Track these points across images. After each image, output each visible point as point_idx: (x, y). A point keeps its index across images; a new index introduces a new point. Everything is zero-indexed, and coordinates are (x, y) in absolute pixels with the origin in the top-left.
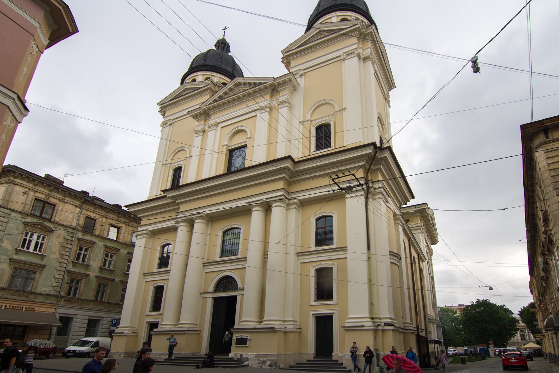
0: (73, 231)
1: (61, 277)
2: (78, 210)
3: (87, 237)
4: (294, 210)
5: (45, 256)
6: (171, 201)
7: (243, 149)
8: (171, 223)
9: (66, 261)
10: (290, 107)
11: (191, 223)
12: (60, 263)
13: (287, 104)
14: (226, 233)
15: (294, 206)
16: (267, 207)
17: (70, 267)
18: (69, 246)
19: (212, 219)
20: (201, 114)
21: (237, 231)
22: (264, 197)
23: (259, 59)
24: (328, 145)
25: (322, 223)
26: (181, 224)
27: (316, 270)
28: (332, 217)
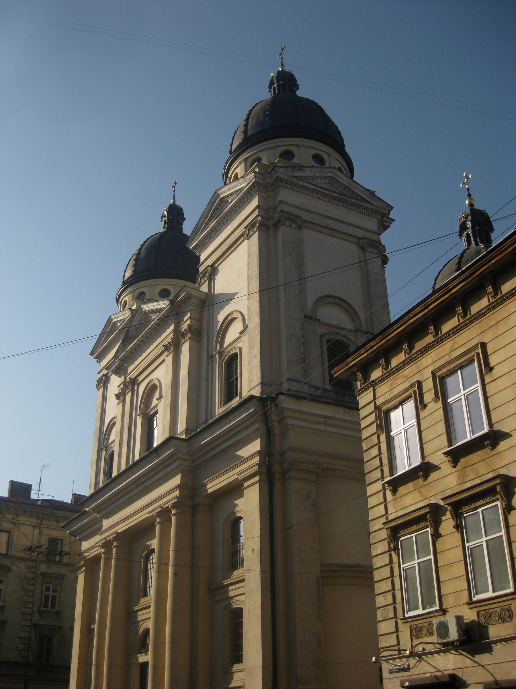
0: (34, 564)
1: (27, 635)
2: (37, 531)
3: (54, 569)
5: (5, 607)
9: (30, 611)
12: (24, 614)
17: (36, 618)
18: (32, 588)
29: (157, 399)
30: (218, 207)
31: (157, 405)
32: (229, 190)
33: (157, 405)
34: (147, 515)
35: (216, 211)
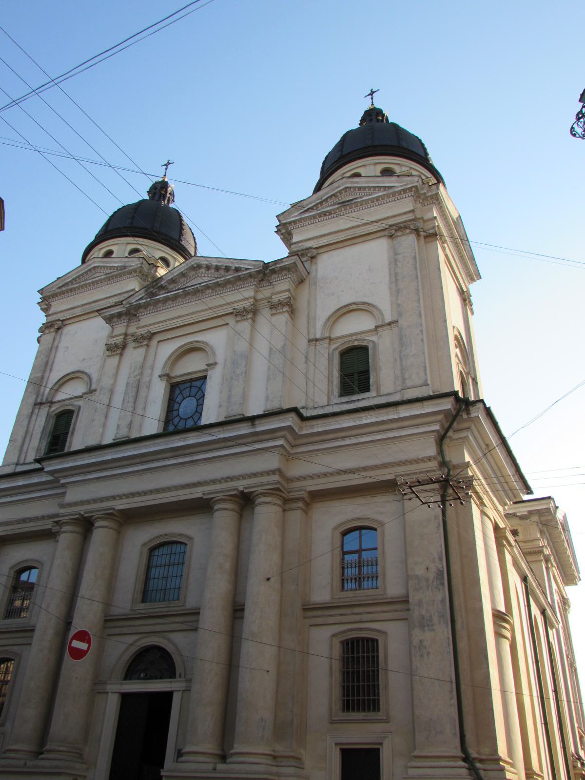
4: (299, 512)
6: (50, 478)
7: (198, 384)
8: (48, 525)
10: (292, 312)
11: (86, 525)
13: (286, 309)
14: (156, 553)
15: (300, 505)
16: (245, 501)
19: (129, 518)
20: (119, 315)
21: (177, 548)
22: (241, 485)
23: (232, 226)
24: (365, 387)
25: (352, 542)
26: (65, 528)
27: (342, 642)
28: (376, 530)
29: (208, 365)
30: (338, 194)
31: (206, 370)
32: (368, 182)
33: (206, 370)
34: (200, 495)
35: (333, 197)
